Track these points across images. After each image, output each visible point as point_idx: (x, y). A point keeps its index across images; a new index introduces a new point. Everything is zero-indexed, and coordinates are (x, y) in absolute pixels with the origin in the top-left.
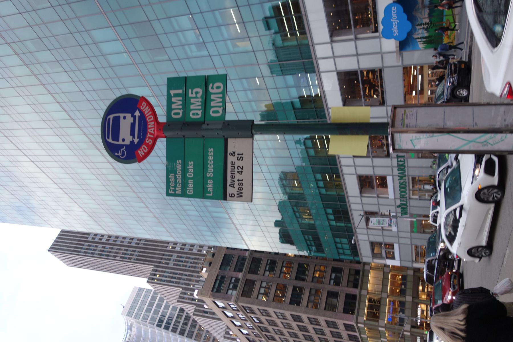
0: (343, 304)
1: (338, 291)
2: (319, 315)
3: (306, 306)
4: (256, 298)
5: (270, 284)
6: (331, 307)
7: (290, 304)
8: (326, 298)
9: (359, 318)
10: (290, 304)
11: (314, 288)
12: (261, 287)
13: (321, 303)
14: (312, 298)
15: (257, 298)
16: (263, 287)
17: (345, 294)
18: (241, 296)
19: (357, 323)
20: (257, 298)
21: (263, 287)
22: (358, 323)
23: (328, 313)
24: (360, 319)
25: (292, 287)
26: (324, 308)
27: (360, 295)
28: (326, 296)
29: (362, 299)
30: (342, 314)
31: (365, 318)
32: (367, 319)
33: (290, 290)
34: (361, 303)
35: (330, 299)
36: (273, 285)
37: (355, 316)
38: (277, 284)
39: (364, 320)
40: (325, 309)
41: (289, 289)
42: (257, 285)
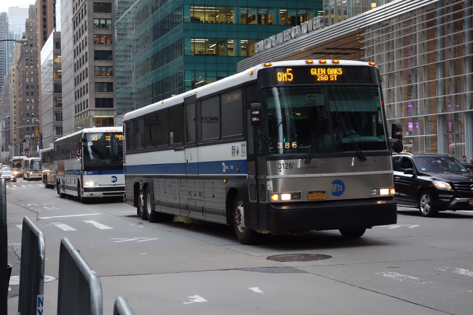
2: (90, 78)
3: (96, 66)
4: (94, 18)
5: (110, 27)
6: (100, 86)
7: (95, 51)
8: (106, 81)
9: (94, 112)
10: (95, 51)
11: (113, 70)
12: (106, 20)
14: (104, 70)
15: (94, 19)
16: (106, 22)
17: (112, 98)
18: (94, 3)
19: (89, 110)
20: (94, 19)
21: (106, 22)
22: (89, 111)
23: (93, 86)
24: (92, 113)
25: (111, 50)
27: (113, 110)
28: (107, 82)
29: (109, 112)
30: (94, 98)
31: (94, 116)
32: (94, 118)
33: (108, 48)
35: (105, 85)
36: (110, 31)
37: (94, 108)
38: (112, 35)
39: (92, 116)
40: (95, 83)
41: (109, 47)
42: (107, 16)
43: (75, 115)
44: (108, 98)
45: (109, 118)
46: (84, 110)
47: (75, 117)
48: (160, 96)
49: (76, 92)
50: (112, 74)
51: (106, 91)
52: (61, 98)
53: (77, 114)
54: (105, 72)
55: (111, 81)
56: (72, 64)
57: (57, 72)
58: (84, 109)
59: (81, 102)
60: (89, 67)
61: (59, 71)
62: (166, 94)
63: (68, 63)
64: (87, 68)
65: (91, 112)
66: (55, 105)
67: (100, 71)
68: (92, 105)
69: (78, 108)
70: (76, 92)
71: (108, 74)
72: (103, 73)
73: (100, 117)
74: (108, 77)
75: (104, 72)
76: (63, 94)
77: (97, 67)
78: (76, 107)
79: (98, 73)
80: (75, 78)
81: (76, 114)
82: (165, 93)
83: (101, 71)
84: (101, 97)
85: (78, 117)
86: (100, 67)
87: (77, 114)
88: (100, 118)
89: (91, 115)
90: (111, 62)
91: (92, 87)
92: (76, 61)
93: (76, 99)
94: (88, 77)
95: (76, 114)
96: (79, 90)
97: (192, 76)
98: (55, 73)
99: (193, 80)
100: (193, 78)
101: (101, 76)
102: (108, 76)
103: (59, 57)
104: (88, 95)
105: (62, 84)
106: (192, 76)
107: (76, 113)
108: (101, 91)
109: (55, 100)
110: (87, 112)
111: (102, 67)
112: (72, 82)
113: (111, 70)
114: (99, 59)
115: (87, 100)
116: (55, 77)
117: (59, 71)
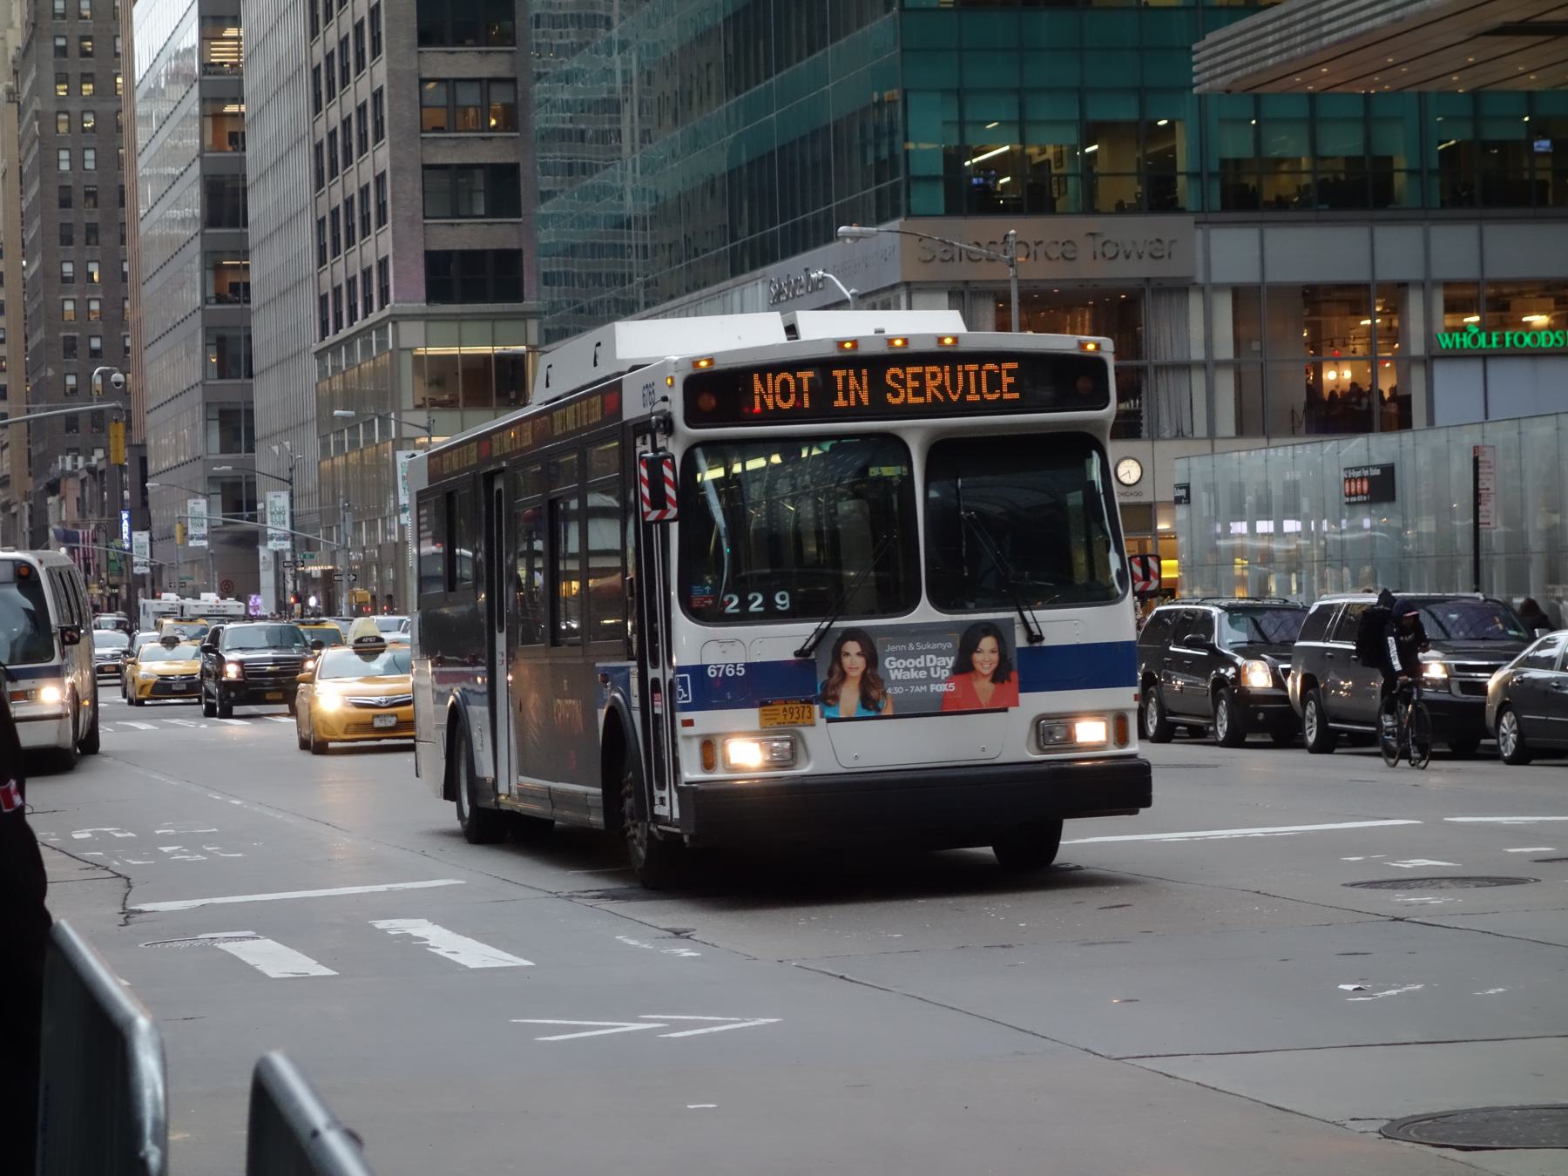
0: (466, 248)
1: (524, 212)
3: (426, 75)
8: (482, 161)
9: (420, 326)
11: (520, 96)
13: (454, 142)
14: (468, 96)
17: (516, 247)
19: (396, 319)
22: (394, 323)
23: (413, 185)
26: (427, 162)
28: (489, 161)
31: (421, 351)
32: (418, 360)
34: (487, 326)
35: (479, 180)
37: (421, 306)
39: (411, 350)
40: (425, 167)
43: (316, 347)
44: (495, 247)
45: (500, 358)
46: (366, 316)
47: (320, 355)
48: (774, 233)
49: (324, 219)
50: (511, 120)
51: (482, 212)
52: (246, 254)
53: (331, 339)
54: (475, 107)
55: (511, 160)
56: (299, 69)
57: (219, 117)
58: (368, 309)
59: (350, 275)
60: (391, 86)
61: (231, 109)
62: (805, 221)
63: (278, 63)
64: (380, 90)
65: (404, 326)
66: (211, 292)
67: (447, 107)
68: (407, 289)
69: (332, 309)
70: (321, 223)
71: (493, 122)
72: (466, 113)
73: (454, 351)
74: (490, 138)
75: (472, 112)
76: (255, 233)
77: (431, 85)
78: (323, 300)
79: (440, 118)
80: (318, 148)
81: (322, 338)
82: (799, 218)
83: (456, 106)
84: (457, 248)
85: (332, 353)
86: (450, 83)
87: (331, 339)
88: (454, 357)
89: (403, 344)
90: (506, 57)
91: (406, 195)
92: (319, 56)
93: (322, 261)
94: (386, 140)
95: (322, 338)
96: (337, 209)
97: (945, 123)
98: (209, 122)
99: (955, 142)
100: (955, 132)
101: (456, 131)
102: (495, 129)
103: (231, 32)
104: (389, 233)
105: (250, 178)
106: (945, 123)
107: (324, 332)
108: (457, 210)
109: (213, 264)
110: (380, 327)
111: (458, 85)
112: (301, 167)
113: (509, 99)
114: (442, 42)
115: (383, 264)
116: (209, 141)
117: (231, 109)
